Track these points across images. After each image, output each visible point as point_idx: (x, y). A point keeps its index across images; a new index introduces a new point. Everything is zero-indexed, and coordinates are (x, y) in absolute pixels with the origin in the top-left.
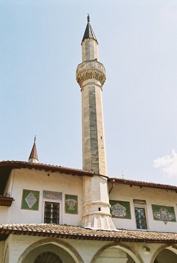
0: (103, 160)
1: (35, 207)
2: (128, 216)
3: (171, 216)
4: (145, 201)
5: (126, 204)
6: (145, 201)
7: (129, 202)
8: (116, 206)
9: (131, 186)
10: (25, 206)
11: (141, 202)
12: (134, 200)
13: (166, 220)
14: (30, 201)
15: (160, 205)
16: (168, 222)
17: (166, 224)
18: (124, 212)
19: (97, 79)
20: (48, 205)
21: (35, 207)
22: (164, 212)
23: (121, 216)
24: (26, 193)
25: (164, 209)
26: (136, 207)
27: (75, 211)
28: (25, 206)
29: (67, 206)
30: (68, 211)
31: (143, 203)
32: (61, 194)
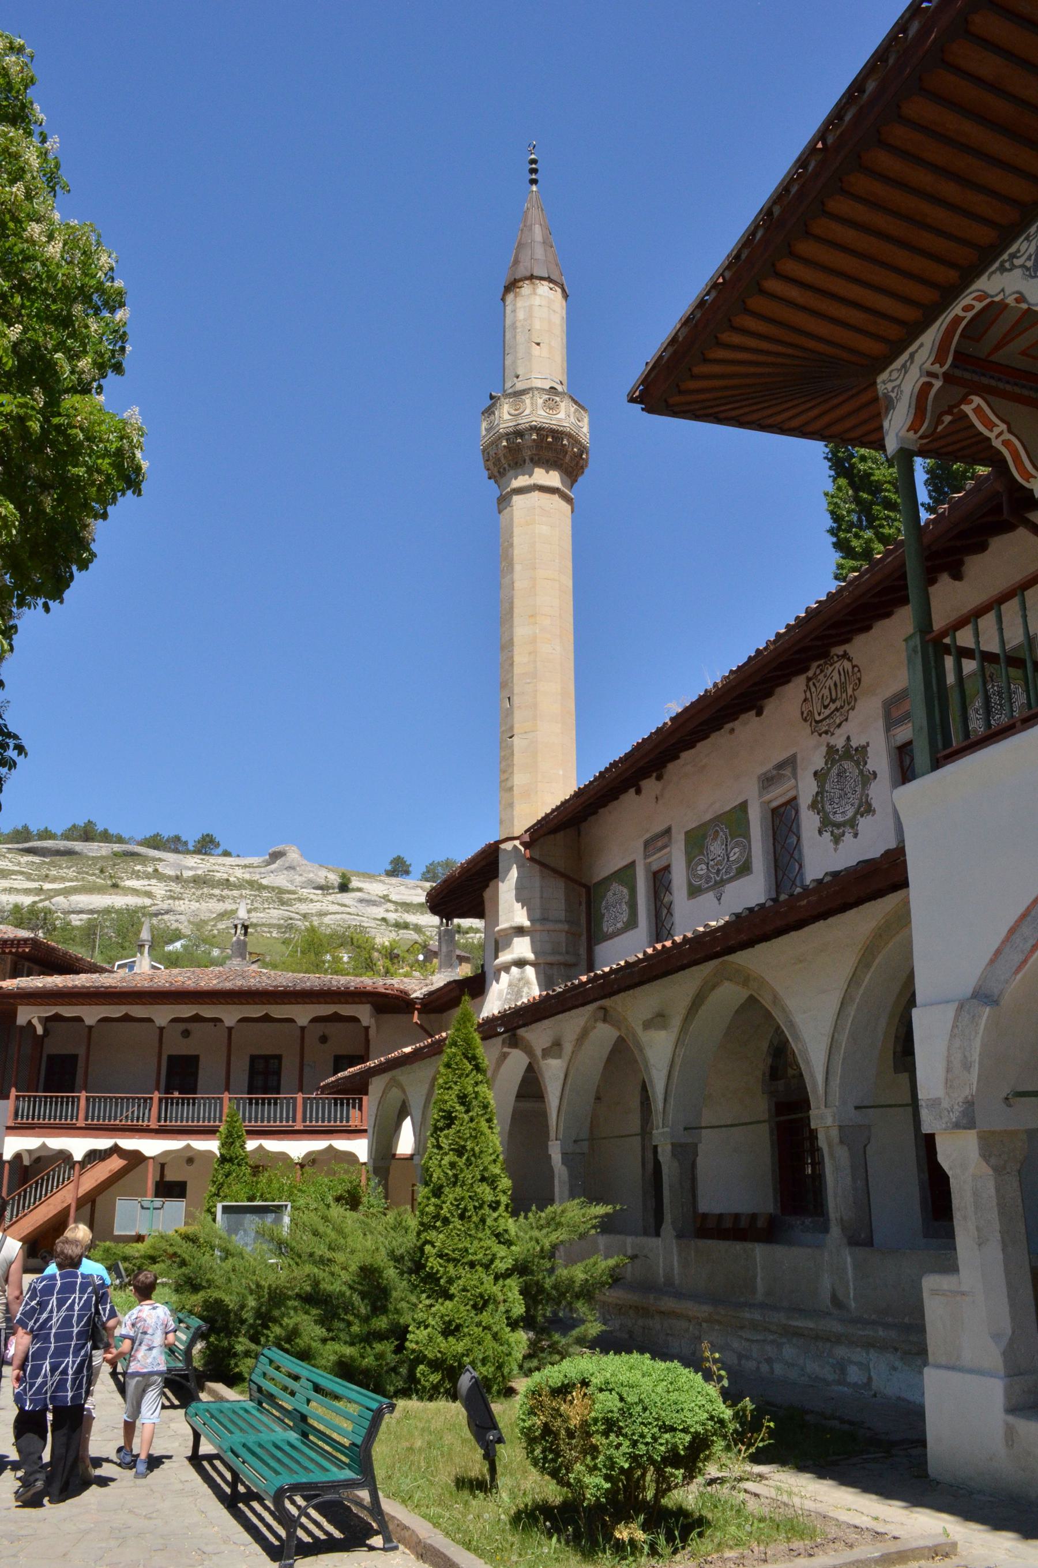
0: (509, 784)
3: (736, 850)
4: (668, 831)
6: (668, 831)
9: (638, 792)
11: (660, 844)
12: (647, 844)
13: (722, 883)
15: (708, 817)
16: (729, 888)
17: (719, 900)
18: (624, 907)
19: (504, 469)
22: (716, 848)
23: (619, 925)
25: (717, 831)
26: (655, 867)
31: (665, 840)
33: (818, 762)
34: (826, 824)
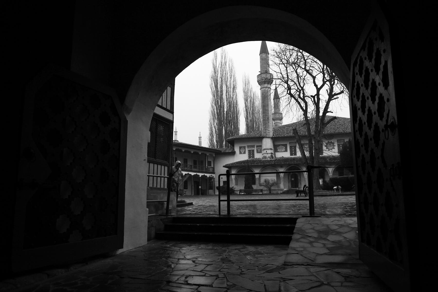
1: (245, 153)
2: (286, 151)
5: (286, 146)
7: (287, 144)
8: (280, 147)
10: (240, 153)
12: (290, 143)
14: (242, 151)
20: (249, 151)
21: (245, 153)
24: (240, 148)
27: (260, 152)
28: (240, 153)
29: (257, 150)
30: (258, 152)
32: (254, 146)
33: (327, 142)
34: (327, 148)
